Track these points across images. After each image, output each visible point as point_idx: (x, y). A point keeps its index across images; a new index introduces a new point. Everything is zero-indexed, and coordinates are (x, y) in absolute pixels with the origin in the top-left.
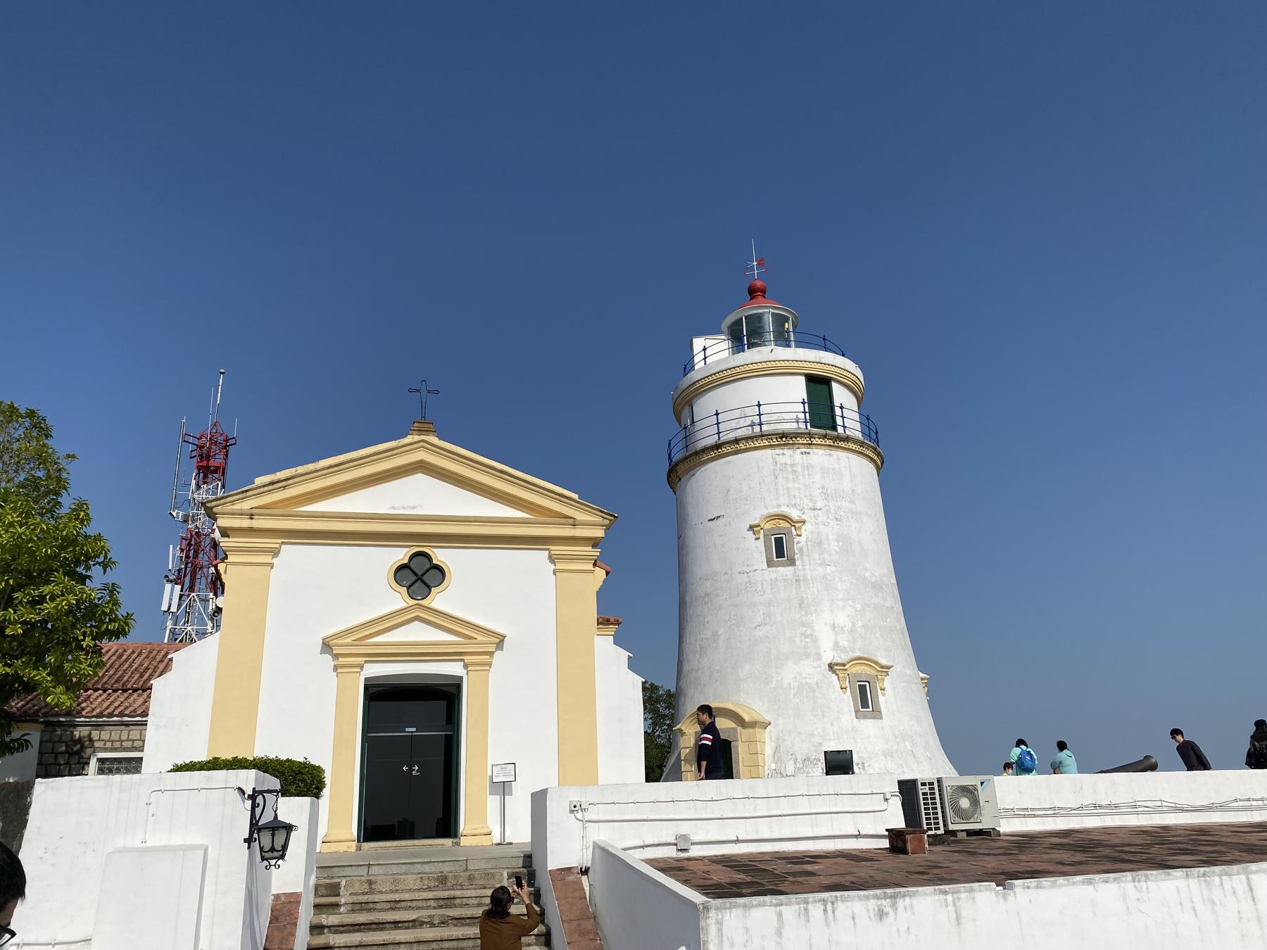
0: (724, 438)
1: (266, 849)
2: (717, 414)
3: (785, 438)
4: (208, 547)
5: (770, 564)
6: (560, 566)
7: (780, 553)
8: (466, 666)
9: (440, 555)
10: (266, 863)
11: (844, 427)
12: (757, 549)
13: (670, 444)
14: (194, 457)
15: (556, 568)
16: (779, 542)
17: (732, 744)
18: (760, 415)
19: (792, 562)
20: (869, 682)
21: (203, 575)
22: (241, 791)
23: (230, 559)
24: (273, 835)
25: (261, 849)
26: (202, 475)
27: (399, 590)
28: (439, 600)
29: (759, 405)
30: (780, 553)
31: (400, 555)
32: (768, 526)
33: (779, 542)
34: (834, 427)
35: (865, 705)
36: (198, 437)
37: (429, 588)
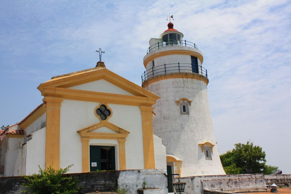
2: (165, 65)
3: (186, 75)
5: (181, 114)
7: (184, 110)
8: (119, 142)
9: (110, 106)
11: (202, 73)
12: (176, 109)
16: (184, 107)
17: (172, 167)
19: (188, 113)
20: (209, 150)
22: (165, 174)
24: (182, 186)
28: (111, 120)
30: (184, 110)
31: (96, 105)
33: (184, 107)
34: (198, 72)
37: (100, 115)
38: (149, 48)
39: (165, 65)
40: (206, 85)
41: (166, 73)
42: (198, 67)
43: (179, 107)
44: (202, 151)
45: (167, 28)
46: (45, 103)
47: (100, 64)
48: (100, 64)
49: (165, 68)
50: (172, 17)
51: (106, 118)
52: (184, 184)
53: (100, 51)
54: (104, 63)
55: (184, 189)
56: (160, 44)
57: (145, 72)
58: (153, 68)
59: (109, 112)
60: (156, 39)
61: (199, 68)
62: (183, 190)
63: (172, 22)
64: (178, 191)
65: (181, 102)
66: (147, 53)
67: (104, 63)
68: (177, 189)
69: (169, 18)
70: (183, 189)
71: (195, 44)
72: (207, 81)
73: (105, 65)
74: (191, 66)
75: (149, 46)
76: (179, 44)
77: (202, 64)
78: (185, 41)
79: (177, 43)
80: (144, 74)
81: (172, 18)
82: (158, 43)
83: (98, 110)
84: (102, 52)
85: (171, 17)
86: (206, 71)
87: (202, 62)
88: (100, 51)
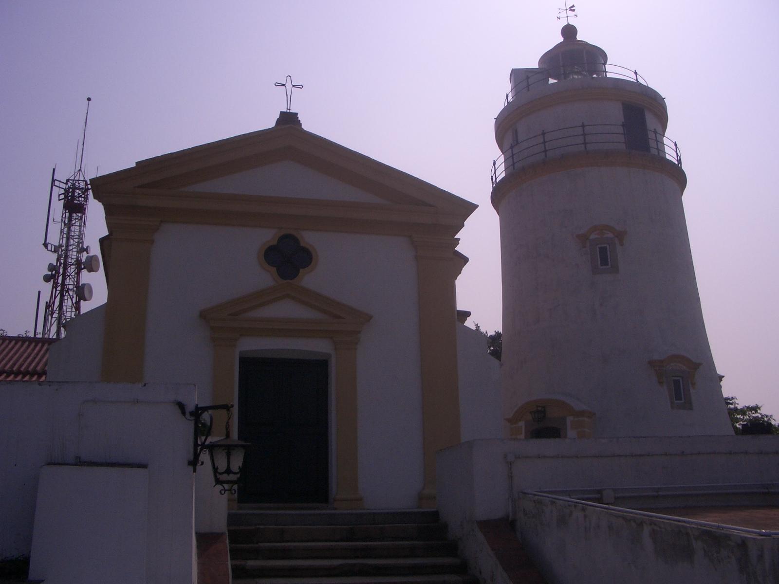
1: (219, 471)
2: (543, 134)
4: (73, 274)
7: (604, 261)
9: (310, 238)
10: (219, 487)
13: (494, 164)
14: (61, 200)
16: (603, 251)
21: (69, 297)
22: (181, 406)
25: (215, 470)
26: (67, 214)
28: (310, 279)
30: (604, 261)
31: (267, 236)
33: (603, 251)
35: (678, 397)
36: (65, 182)
39: (543, 134)
41: (546, 156)
44: (660, 383)
50: (572, 9)
51: (294, 275)
54: (297, 114)
65: (593, 236)
67: (297, 114)
69: (564, 14)
71: (636, 73)
74: (621, 130)
81: (574, 10)
85: (570, 10)
86: (676, 145)
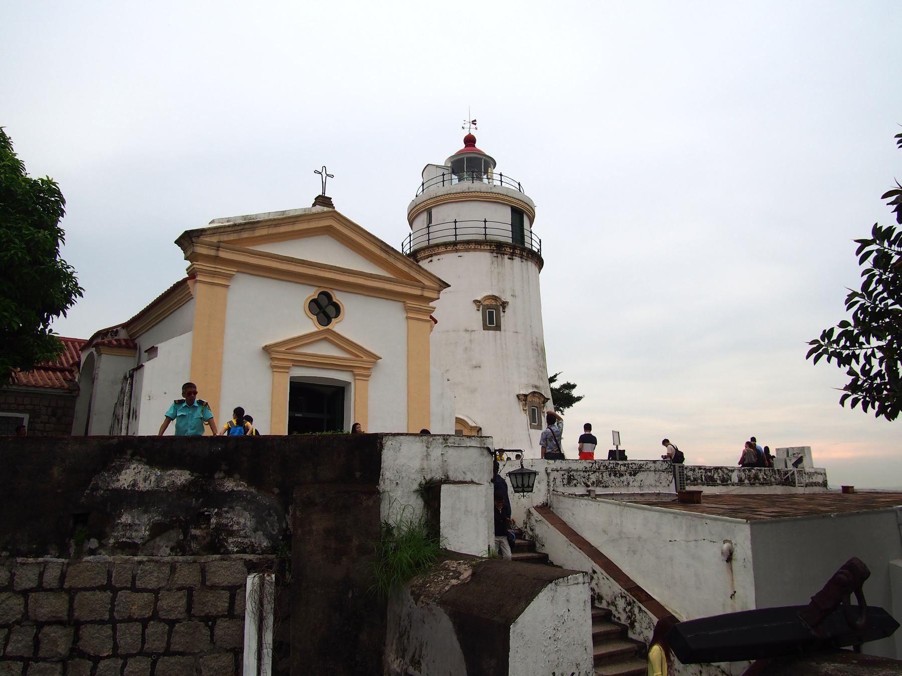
0: (459, 238)
5: (485, 328)
6: (410, 315)
8: (355, 375)
9: (338, 297)
11: (532, 245)
15: (409, 315)
18: (485, 228)
19: (498, 328)
23: (198, 278)
27: (311, 317)
28: (338, 326)
29: (485, 221)
30: (491, 322)
31: (311, 293)
32: (486, 303)
38: (423, 184)
40: (538, 271)
42: (523, 232)
43: (480, 314)
45: (463, 146)
46: (192, 274)
47: (323, 200)
48: (323, 200)
49: (456, 229)
50: (474, 122)
51: (329, 321)
52: (534, 475)
53: (324, 173)
55: (533, 485)
56: (446, 177)
57: (410, 235)
58: (428, 227)
59: (337, 309)
60: (437, 166)
61: (526, 233)
62: (530, 489)
63: (474, 133)
64: (520, 489)
66: (417, 196)
68: (515, 486)
69: (467, 126)
70: (531, 485)
71: (519, 184)
72: (539, 262)
73: (333, 205)
74: (510, 228)
75: (421, 181)
76: (485, 181)
77: (531, 227)
78: (501, 175)
79: (481, 179)
80: (408, 240)
81: (475, 124)
82: (443, 175)
83: (313, 303)
84: (328, 175)
86: (540, 242)
87: (531, 222)
88: (324, 173)
